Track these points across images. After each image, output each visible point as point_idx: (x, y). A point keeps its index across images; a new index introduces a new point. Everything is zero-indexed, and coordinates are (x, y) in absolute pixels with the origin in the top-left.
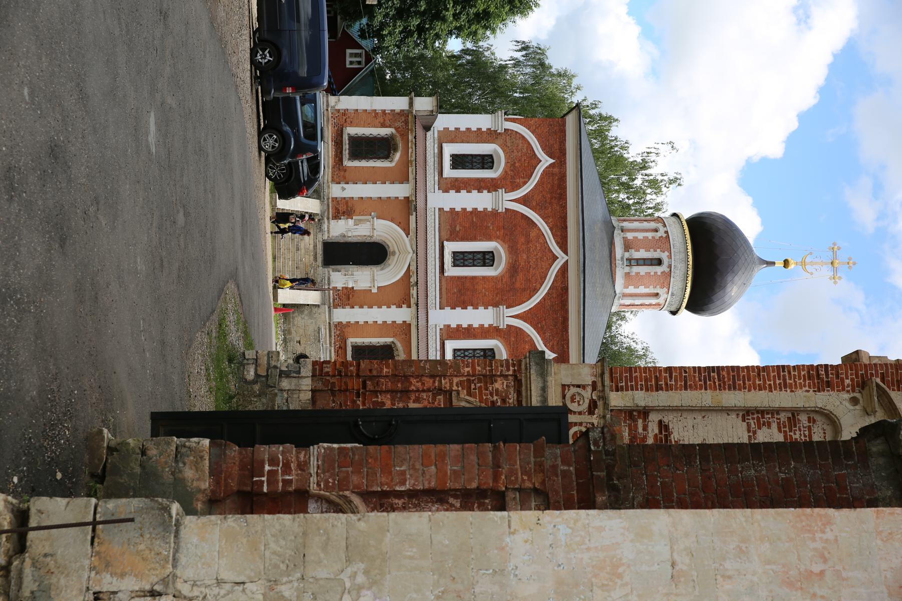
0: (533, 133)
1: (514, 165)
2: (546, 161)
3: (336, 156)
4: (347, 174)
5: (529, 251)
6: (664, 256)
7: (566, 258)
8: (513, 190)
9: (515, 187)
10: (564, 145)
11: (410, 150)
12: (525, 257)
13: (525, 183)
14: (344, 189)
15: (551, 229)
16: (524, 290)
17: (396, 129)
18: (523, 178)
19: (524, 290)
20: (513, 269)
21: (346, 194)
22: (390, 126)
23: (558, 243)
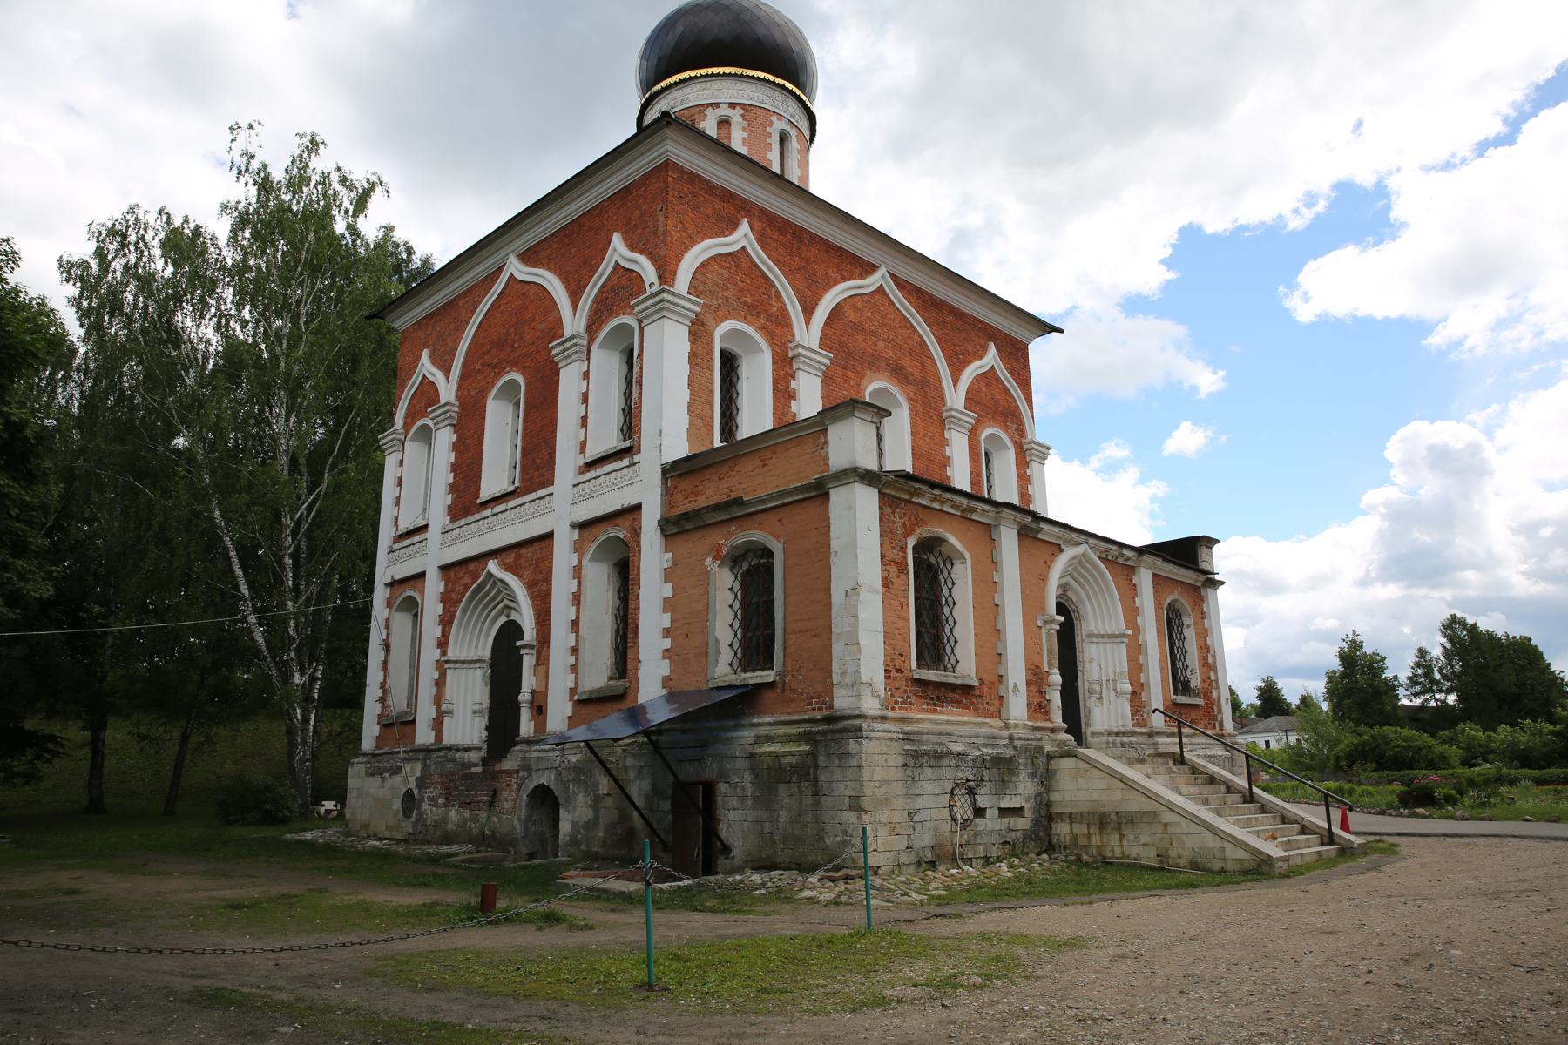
0: (694, 243)
1: (750, 307)
2: (742, 237)
3: (958, 703)
4: (988, 678)
5: (874, 334)
6: (778, 125)
7: (882, 271)
8: (789, 326)
9: (783, 320)
10: (716, 187)
11: (947, 508)
12: (881, 344)
13: (779, 296)
14: (1016, 689)
15: (844, 279)
16: (922, 364)
17: (907, 534)
18: (770, 298)
19: (922, 364)
20: (899, 374)
21: (1023, 687)
22: (903, 549)
23: (861, 277)
